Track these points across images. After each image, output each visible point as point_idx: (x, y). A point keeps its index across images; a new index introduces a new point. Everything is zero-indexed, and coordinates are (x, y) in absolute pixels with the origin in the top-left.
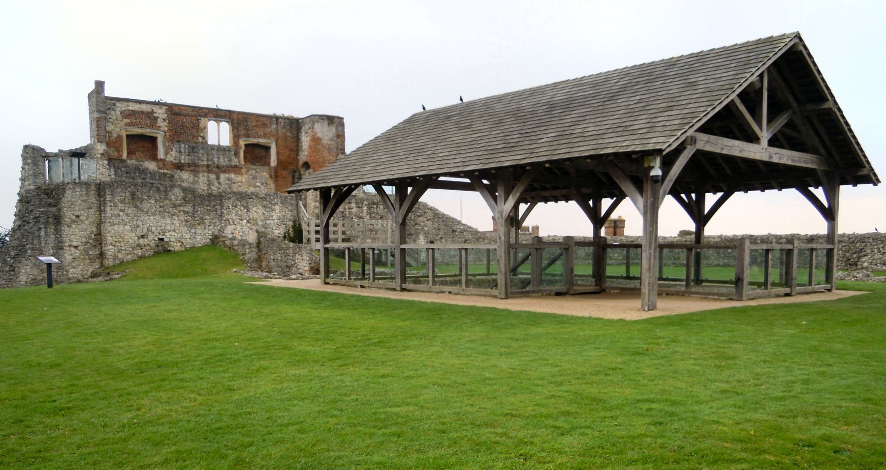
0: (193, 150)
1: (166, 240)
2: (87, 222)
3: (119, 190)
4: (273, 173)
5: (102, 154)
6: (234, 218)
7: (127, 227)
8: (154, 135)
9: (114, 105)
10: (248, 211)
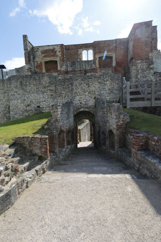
0: (73, 64)
1: (41, 107)
2: (4, 100)
3: (13, 81)
4: (114, 70)
5: (27, 69)
6: (80, 91)
7: (19, 101)
8: (56, 60)
9: (38, 49)
10: (89, 86)
